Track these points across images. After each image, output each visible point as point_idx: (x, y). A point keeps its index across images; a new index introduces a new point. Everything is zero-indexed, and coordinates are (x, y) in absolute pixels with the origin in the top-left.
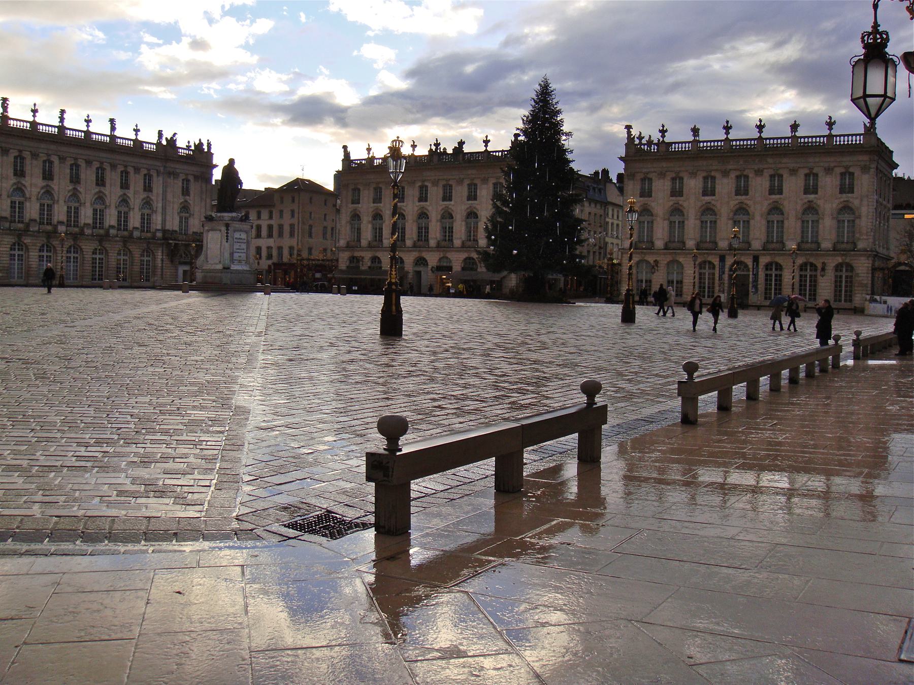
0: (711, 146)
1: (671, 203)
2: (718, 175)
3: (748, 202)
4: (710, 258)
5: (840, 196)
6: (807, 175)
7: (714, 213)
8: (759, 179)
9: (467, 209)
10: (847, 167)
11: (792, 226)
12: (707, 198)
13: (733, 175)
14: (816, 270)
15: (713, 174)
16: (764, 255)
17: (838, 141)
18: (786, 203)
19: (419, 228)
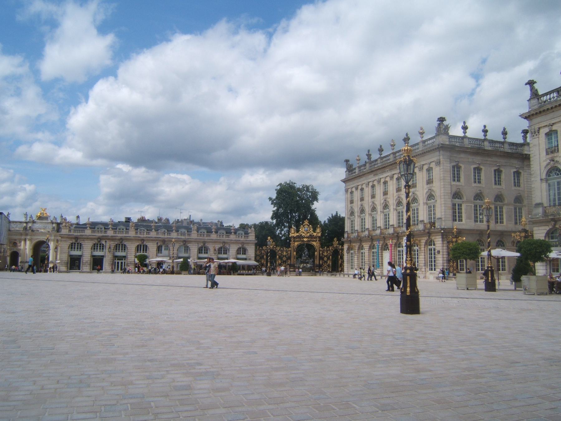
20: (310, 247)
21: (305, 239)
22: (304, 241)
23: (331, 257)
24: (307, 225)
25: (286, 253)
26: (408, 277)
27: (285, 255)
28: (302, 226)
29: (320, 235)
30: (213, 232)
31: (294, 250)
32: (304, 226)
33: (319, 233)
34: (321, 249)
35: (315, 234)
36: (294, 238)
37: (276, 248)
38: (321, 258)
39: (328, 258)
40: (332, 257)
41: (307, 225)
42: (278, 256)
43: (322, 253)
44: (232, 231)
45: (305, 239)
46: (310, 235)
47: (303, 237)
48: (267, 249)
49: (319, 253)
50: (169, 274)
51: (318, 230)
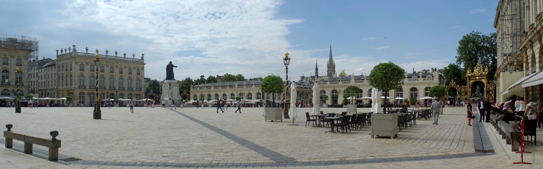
0: (92, 56)
1: (90, 74)
2: (105, 66)
3: (114, 75)
4: (104, 92)
5: (137, 75)
6: (129, 69)
7: (113, 78)
8: (117, 68)
9: (3, 68)
10: (138, 68)
11: (134, 83)
12: (102, 73)
13: (109, 67)
14: (94, 95)
15: (104, 66)
16: (119, 91)
17: (125, 59)
18: (124, 76)
19: (2, 77)
20: (481, 84)
21: (477, 78)
22: (476, 79)
23: (448, 93)
24: (479, 66)
25: (464, 89)
26: (97, 105)
27: (463, 91)
28: (475, 67)
29: (487, 73)
30: (406, 77)
31: (469, 87)
32: (476, 67)
33: (486, 72)
34: (488, 85)
35: (484, 73)
36: (469, 77)
37: (456, 86)
38: (488, 92)
39: (492, 92)
40: (448, 93)
41: (479, 66)
42: (457, 93)
43: (489, 88)
44: (420, 76)
45: (477, 78)
46: (481, 74)
47: (476, 76)
48: (449, 87)
49: (487, 88)
50: (366, 107)
51: (486, 70)
